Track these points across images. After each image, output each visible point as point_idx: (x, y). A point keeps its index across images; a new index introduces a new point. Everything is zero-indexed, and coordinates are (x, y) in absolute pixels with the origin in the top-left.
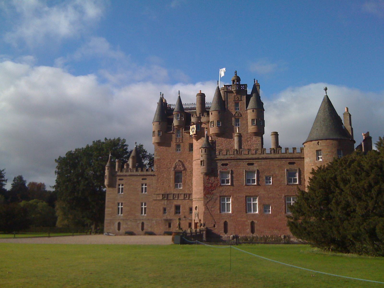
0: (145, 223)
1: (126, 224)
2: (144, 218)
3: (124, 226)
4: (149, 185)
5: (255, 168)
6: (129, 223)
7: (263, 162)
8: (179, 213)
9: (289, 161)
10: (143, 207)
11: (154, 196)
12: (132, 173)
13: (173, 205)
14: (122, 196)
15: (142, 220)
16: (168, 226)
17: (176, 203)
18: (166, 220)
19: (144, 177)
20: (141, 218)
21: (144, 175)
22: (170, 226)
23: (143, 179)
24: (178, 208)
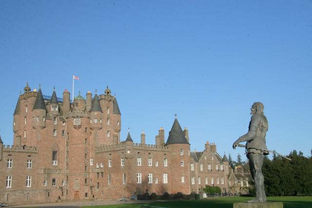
0: (31, 193)
1: (15, 195)
2: (30, 189)
3: (13, 197)
4: (33, 162)
5: (151, 155)
6: (17, 194)
7: (155, 153)
8: (55, 184)
9: (165, 153)
10: (28, 180)
11: (37, 170)
12: (20, 150)
13: (52, 178)
14: (11, 170)
15: (28, 190)
16: (47, 195)
17: (53, 176)
18: (46, 190)
19: (30, 154)
20: (27, 189)
21: (29, 152)
22: (49, 196)
23: (29, 156)
24: (54, 180)
